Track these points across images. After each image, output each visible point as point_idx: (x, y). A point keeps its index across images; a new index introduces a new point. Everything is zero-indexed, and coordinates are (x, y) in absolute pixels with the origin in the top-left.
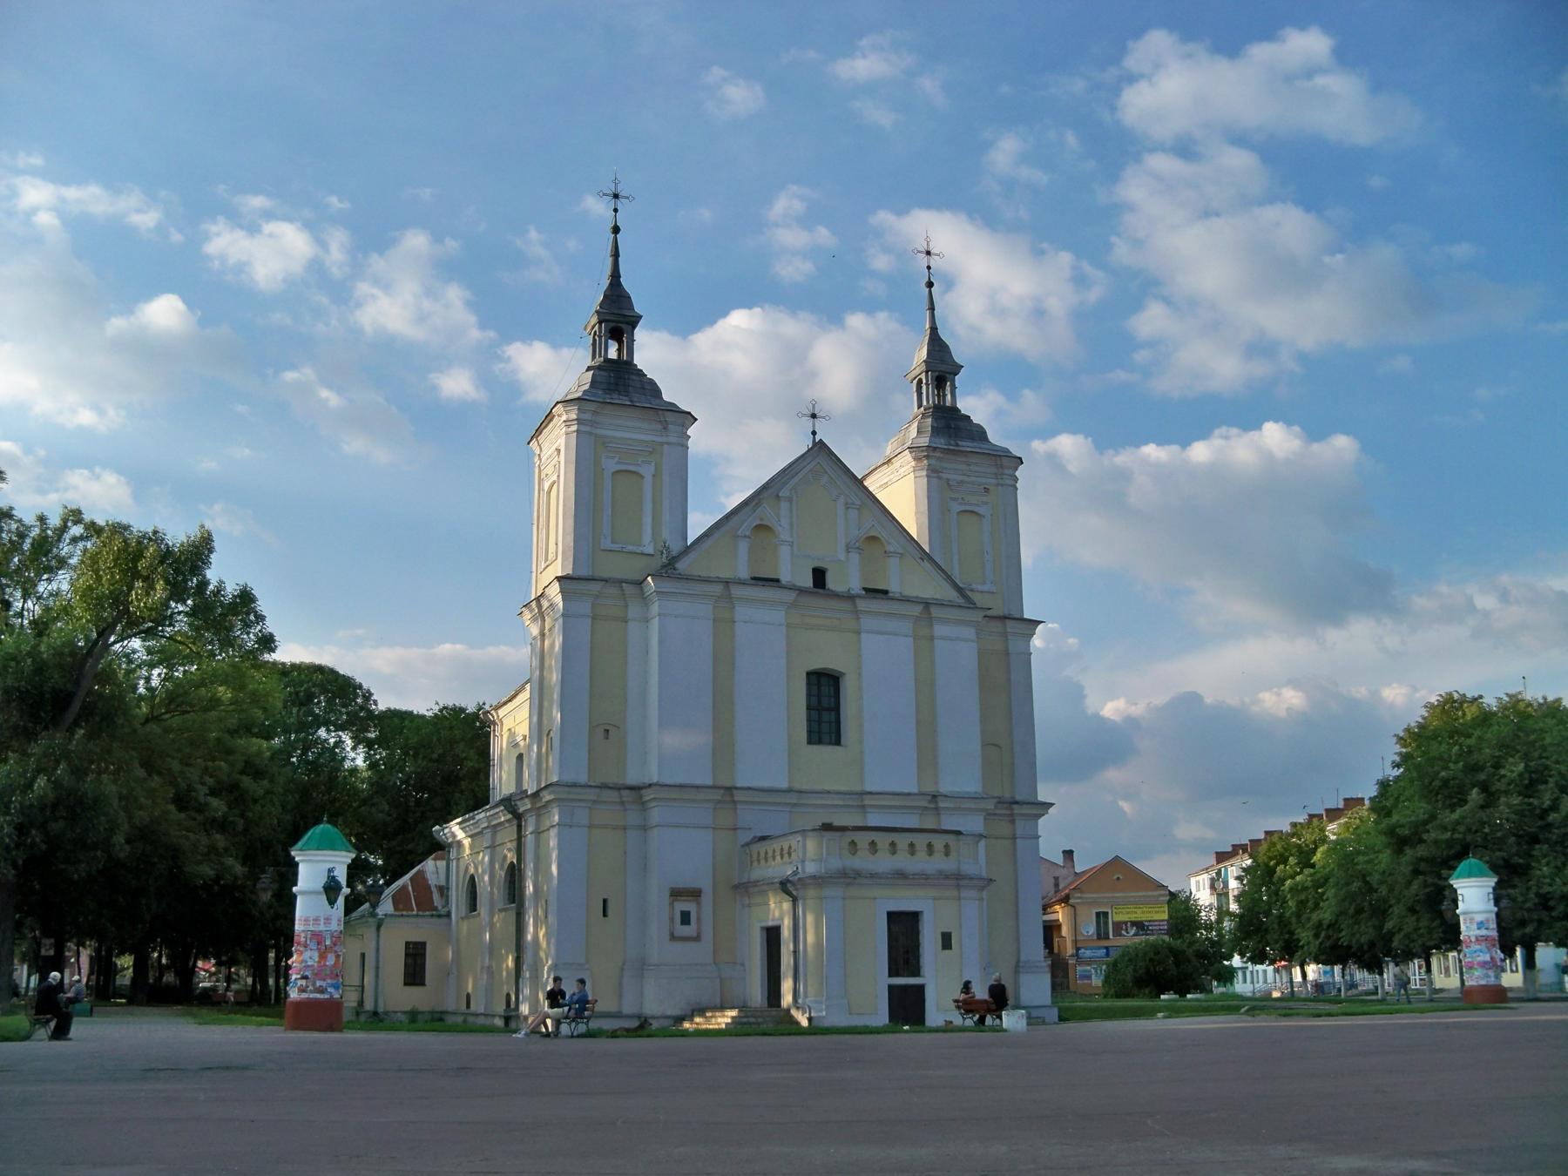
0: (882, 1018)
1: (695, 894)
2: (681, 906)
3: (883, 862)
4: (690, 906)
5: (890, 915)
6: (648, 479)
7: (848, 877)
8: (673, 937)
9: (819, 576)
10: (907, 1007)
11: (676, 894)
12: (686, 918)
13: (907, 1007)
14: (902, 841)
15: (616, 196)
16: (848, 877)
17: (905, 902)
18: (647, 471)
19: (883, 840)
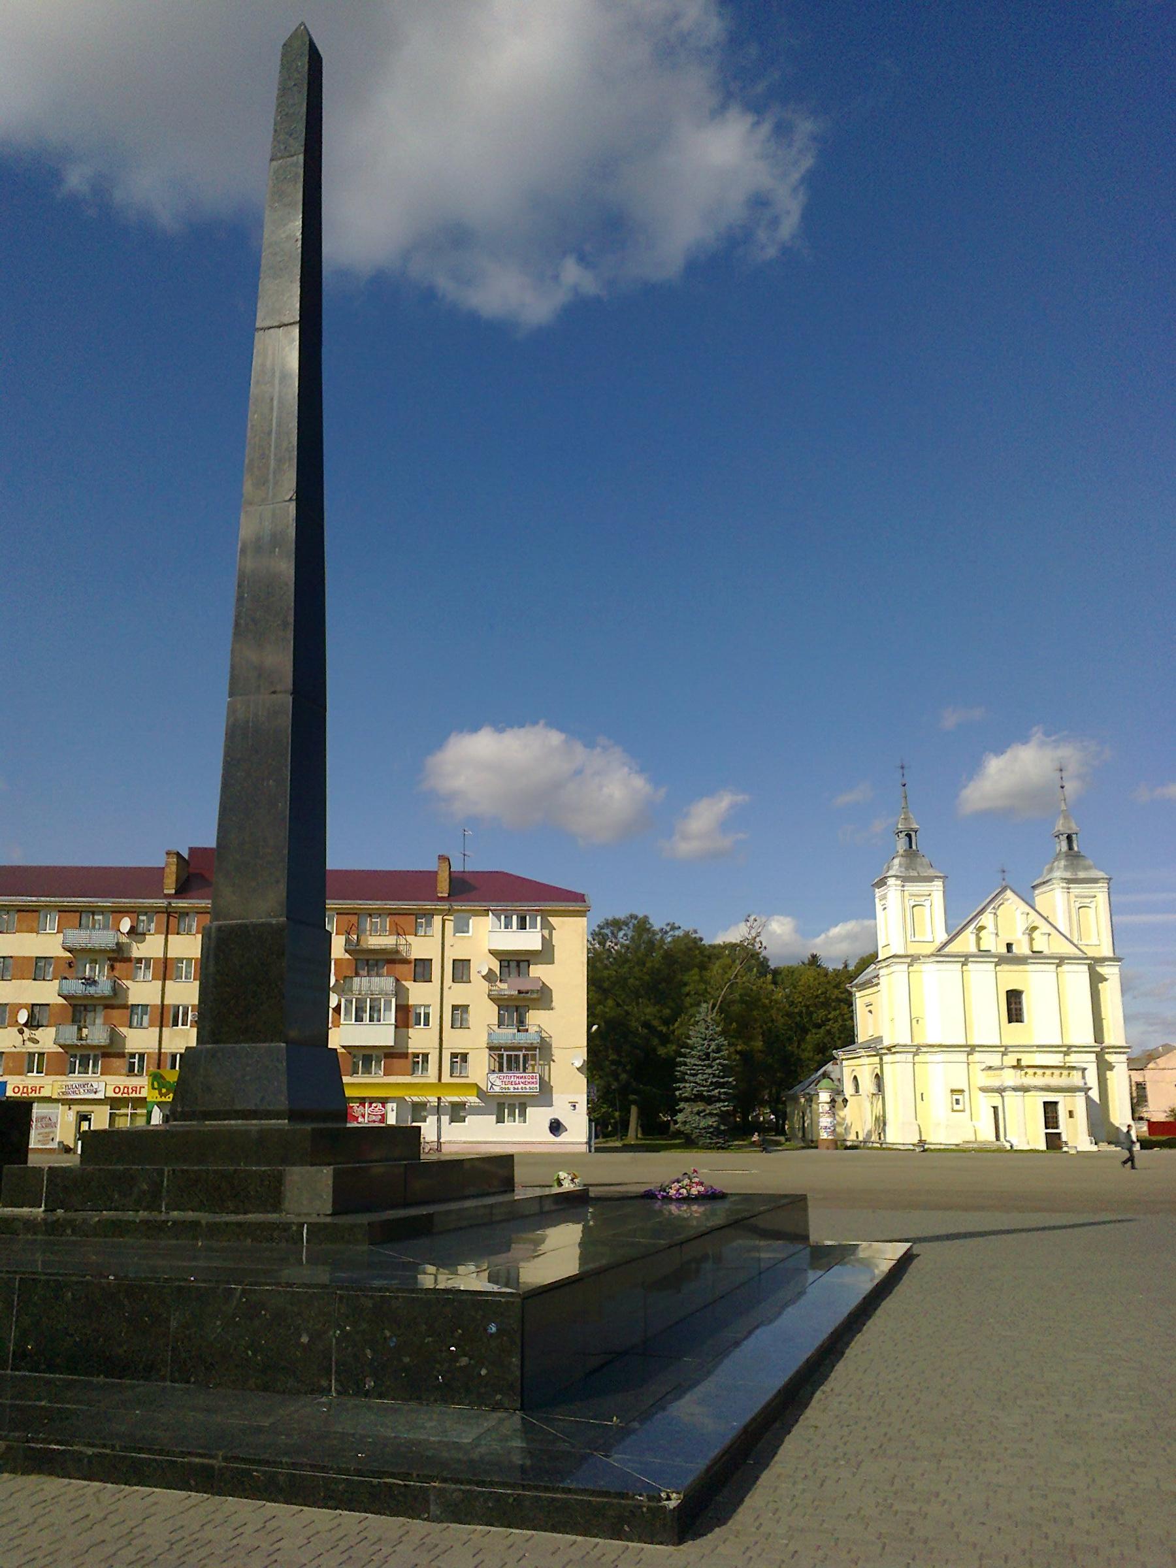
0: (1043, 1147)
1: (963, 1091)
2: (955, 1097)
3: (1039, 1081)
4: (960, 1097)
5: (1045, 1103)
6: (927, 910)
7: (1025, 1089)
8: (953, 1111)
9: (1009, 946)
10: (1054, 1141)
11: (952, 1091)
12: (957, 1101)
13: (1054, 1141)
14: (1048, 1072)
15: (902, 768)
16: (1025, 1089)
17: (1051, 1097)
18: (927, 903)
19: (1040, 1072)
